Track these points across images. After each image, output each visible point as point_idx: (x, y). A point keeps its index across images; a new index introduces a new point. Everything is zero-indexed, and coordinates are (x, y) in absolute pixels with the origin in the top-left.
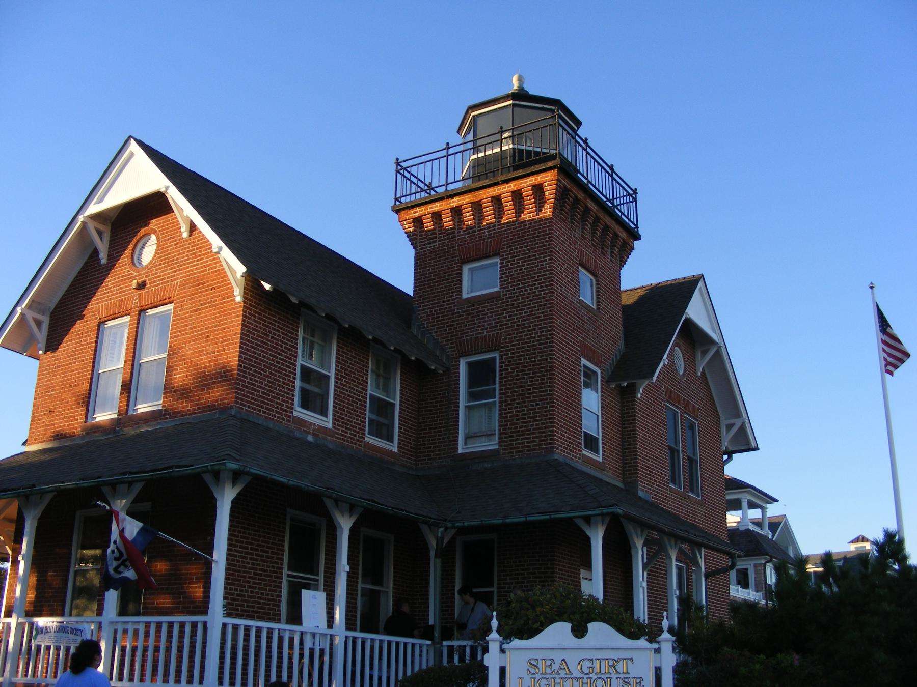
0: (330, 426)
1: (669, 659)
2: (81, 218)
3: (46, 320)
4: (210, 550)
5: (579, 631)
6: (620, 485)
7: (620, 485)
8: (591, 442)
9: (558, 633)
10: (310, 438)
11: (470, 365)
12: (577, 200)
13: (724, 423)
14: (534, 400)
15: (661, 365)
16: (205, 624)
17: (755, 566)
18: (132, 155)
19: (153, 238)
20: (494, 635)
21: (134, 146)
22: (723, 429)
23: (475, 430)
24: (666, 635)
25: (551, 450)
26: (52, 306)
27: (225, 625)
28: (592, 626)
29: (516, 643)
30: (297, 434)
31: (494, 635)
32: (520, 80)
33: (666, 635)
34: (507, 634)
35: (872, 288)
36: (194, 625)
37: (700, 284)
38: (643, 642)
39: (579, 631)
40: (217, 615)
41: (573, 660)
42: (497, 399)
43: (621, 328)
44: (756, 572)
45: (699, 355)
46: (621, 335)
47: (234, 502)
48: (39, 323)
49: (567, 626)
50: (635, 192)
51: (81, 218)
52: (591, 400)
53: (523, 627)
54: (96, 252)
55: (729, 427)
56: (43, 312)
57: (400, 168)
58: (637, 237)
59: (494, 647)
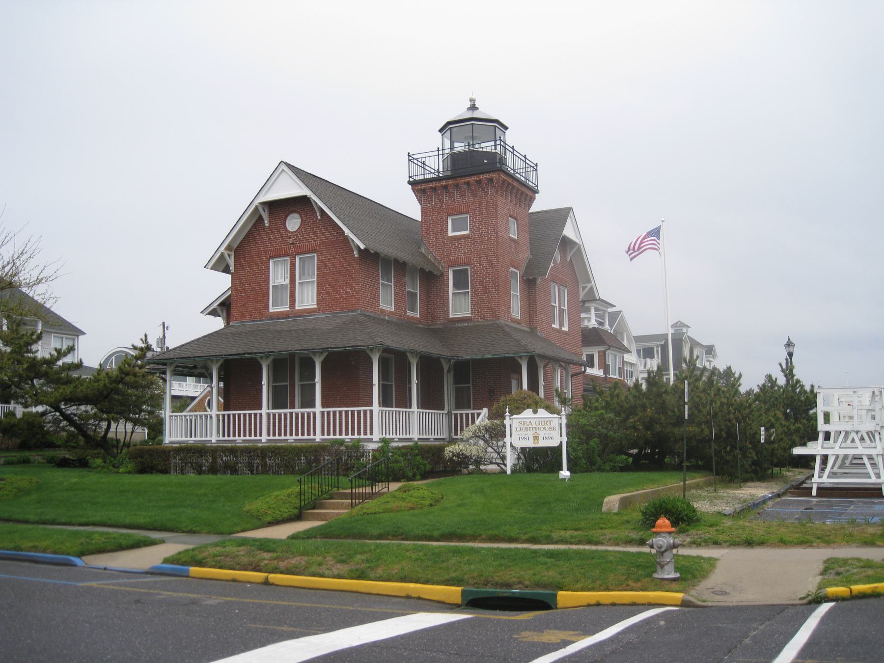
1: (564, 421)
2: (257, 202)
3: (233, 254)
5: (535, 412)
6: (528, 330)
7: (528, 330)
9: (528, 413)
10: (387, 318)
12: (509, 184)
13: (581, 285)
14: (489, 293)
16: (371, 411)
17: (599, 352)
20: (507, 414)
21: (284, 167)
22: (581, 289)
23: (458, 306)
25: (498, 318)
29: (515, 416)
30: (382, 317)
31: (507, 414)
34: (512, 414)
36: (365, 412)
37: (571, 213)
38: (556, 416)
39: (535, 412)
40: (376, 407)
41: (533, 421)
42: (469, 290)
48: (229, 256)
49: (531, 410)
50: (536, 165)
53: (517, 409)
55: (584, 288)
57: (411, 158)
59: (507, 418)
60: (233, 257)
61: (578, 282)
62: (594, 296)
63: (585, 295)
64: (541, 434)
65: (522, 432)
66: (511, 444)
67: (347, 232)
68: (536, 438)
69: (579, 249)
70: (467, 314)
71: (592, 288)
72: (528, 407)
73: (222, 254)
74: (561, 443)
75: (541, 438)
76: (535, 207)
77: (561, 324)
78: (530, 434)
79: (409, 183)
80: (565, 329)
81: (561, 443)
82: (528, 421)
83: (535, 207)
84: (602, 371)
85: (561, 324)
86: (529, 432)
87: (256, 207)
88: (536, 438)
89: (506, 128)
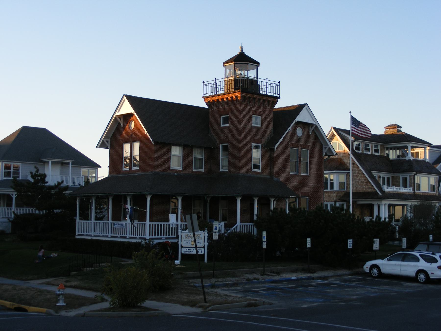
0: (182, 169)
2: (114, 116)
3: (109, 140)
4: (146, 209)
7: (268, 177)
8: (256, 167)
10: (176, 174)
11: (223, 146)
13: (324, 147)
15: (280, 141)
17: (410, 176)
18: (125, 100)
19: (133, 122)
22: (324, 149)
24: (206, 231)
26: (111, 136)
27: (150, 225)
29: (183, 231)
32: (242, 48)
33: (206, 231)
35: (350, 113)
38: (203, 232)
40: (148, 222)
43: (272, 128)
44: (410, 179)
46: (272, 130)
47: (150, 199)
48: (107, 141)
51: (114, 116)
52: (256, 154)
54: (119, 124)
55: (326, 148)
56: (108, 139)
58: (279, 98)
60: (109, 142)
61: (322, 145)
62: (332, 153)
69: (316, 126)
70: (226, 170)
71: (329, 148)
73: (103, 141)
76: (278, 106)
79: (203, 97)
83: (278, 106)
84: (411, 188)
89: (258, 63)
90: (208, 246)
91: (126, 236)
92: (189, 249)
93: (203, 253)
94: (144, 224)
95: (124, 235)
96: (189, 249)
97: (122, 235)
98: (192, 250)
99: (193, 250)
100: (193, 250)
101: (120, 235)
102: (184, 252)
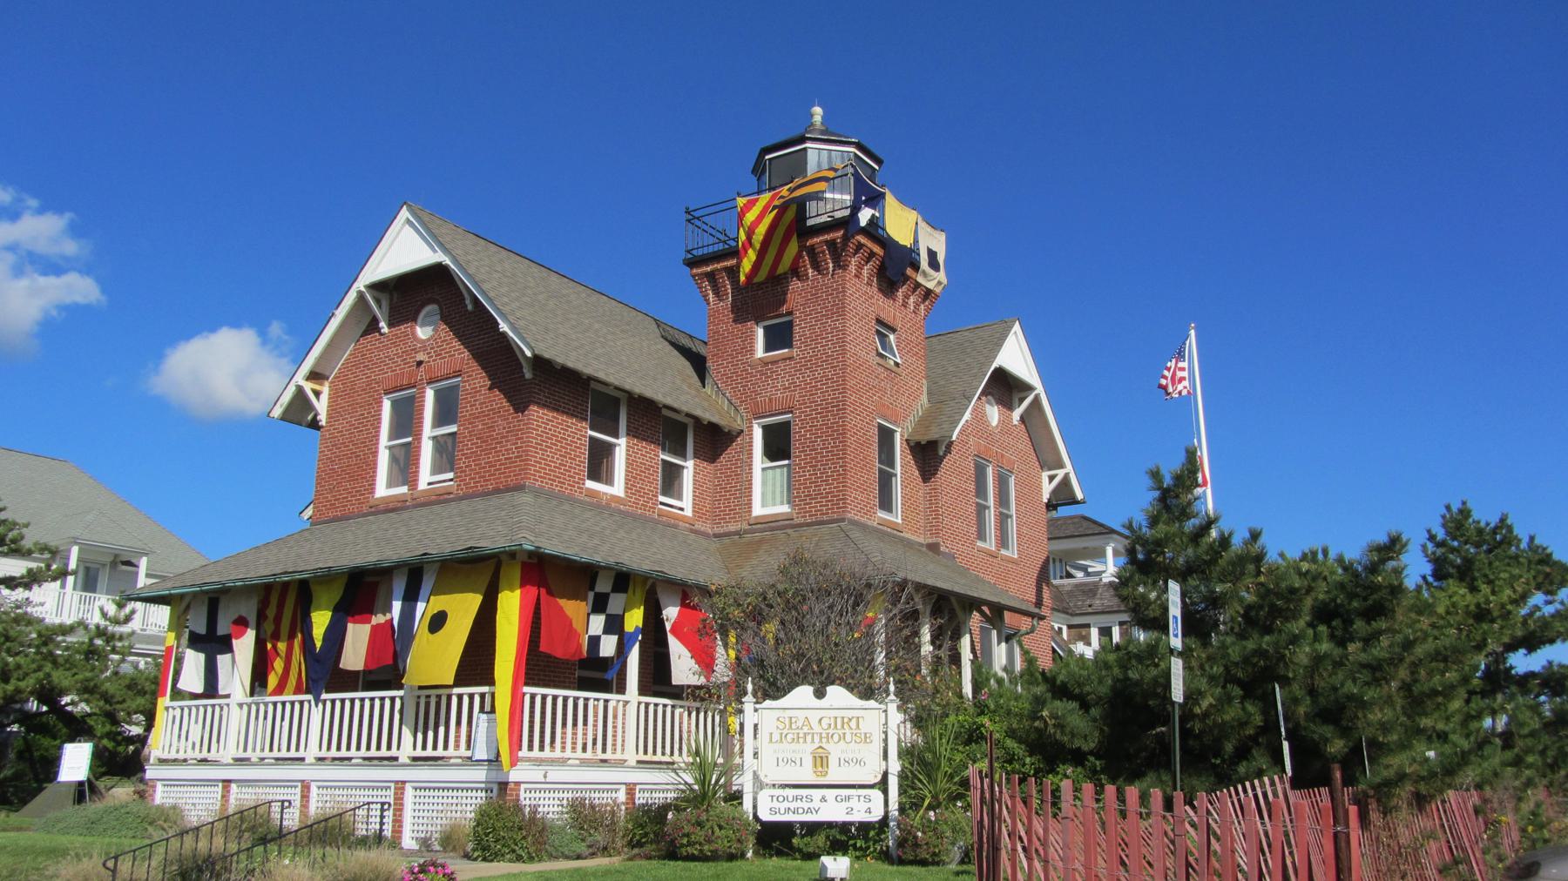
3: (325, 390)
5: (820, 694)
9: (803, 694)
24: (892, 697)
28: (831, 689)
29: (768, 703)
33: (892, 697)
38: (872, 703)
39: (820, 694)
41: (814, 717)
45: (1016, 401)
53: (772, 689)
55: (1051, 478)
57: (692, 217)
63: (1054, 492)
64: (835, 751)
65: (785, 745)
66: (756, 775)
67: (504, 327)
68: (821, 760)
72: (805, 681)
74: (885, 775)
75: (833, 761)
77: (1003, 541)
78: (806, 750)
80: (1012, 552)
81: (885, 775)
82: (801, 715)
85: (1003, 541)
86: (800, 746)
87: (361, 296)
88: (821, 760)
90: (902, 776)
91: (394, 752)
92: (796, 798)
93: (876, 815)
94: (482, 696)
95: (384, 752)
96: (796, 798)
97: (373, 753)
98: (816, 804)
99: (823, 799)
100: (823, 799)
101: (363, 752)
102: (773, 811)
